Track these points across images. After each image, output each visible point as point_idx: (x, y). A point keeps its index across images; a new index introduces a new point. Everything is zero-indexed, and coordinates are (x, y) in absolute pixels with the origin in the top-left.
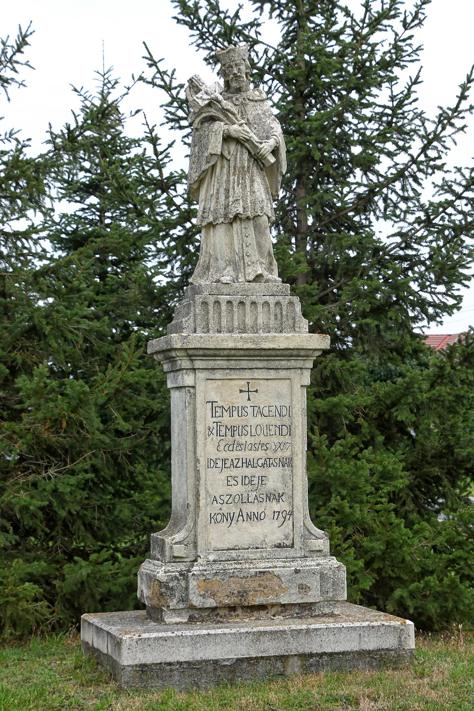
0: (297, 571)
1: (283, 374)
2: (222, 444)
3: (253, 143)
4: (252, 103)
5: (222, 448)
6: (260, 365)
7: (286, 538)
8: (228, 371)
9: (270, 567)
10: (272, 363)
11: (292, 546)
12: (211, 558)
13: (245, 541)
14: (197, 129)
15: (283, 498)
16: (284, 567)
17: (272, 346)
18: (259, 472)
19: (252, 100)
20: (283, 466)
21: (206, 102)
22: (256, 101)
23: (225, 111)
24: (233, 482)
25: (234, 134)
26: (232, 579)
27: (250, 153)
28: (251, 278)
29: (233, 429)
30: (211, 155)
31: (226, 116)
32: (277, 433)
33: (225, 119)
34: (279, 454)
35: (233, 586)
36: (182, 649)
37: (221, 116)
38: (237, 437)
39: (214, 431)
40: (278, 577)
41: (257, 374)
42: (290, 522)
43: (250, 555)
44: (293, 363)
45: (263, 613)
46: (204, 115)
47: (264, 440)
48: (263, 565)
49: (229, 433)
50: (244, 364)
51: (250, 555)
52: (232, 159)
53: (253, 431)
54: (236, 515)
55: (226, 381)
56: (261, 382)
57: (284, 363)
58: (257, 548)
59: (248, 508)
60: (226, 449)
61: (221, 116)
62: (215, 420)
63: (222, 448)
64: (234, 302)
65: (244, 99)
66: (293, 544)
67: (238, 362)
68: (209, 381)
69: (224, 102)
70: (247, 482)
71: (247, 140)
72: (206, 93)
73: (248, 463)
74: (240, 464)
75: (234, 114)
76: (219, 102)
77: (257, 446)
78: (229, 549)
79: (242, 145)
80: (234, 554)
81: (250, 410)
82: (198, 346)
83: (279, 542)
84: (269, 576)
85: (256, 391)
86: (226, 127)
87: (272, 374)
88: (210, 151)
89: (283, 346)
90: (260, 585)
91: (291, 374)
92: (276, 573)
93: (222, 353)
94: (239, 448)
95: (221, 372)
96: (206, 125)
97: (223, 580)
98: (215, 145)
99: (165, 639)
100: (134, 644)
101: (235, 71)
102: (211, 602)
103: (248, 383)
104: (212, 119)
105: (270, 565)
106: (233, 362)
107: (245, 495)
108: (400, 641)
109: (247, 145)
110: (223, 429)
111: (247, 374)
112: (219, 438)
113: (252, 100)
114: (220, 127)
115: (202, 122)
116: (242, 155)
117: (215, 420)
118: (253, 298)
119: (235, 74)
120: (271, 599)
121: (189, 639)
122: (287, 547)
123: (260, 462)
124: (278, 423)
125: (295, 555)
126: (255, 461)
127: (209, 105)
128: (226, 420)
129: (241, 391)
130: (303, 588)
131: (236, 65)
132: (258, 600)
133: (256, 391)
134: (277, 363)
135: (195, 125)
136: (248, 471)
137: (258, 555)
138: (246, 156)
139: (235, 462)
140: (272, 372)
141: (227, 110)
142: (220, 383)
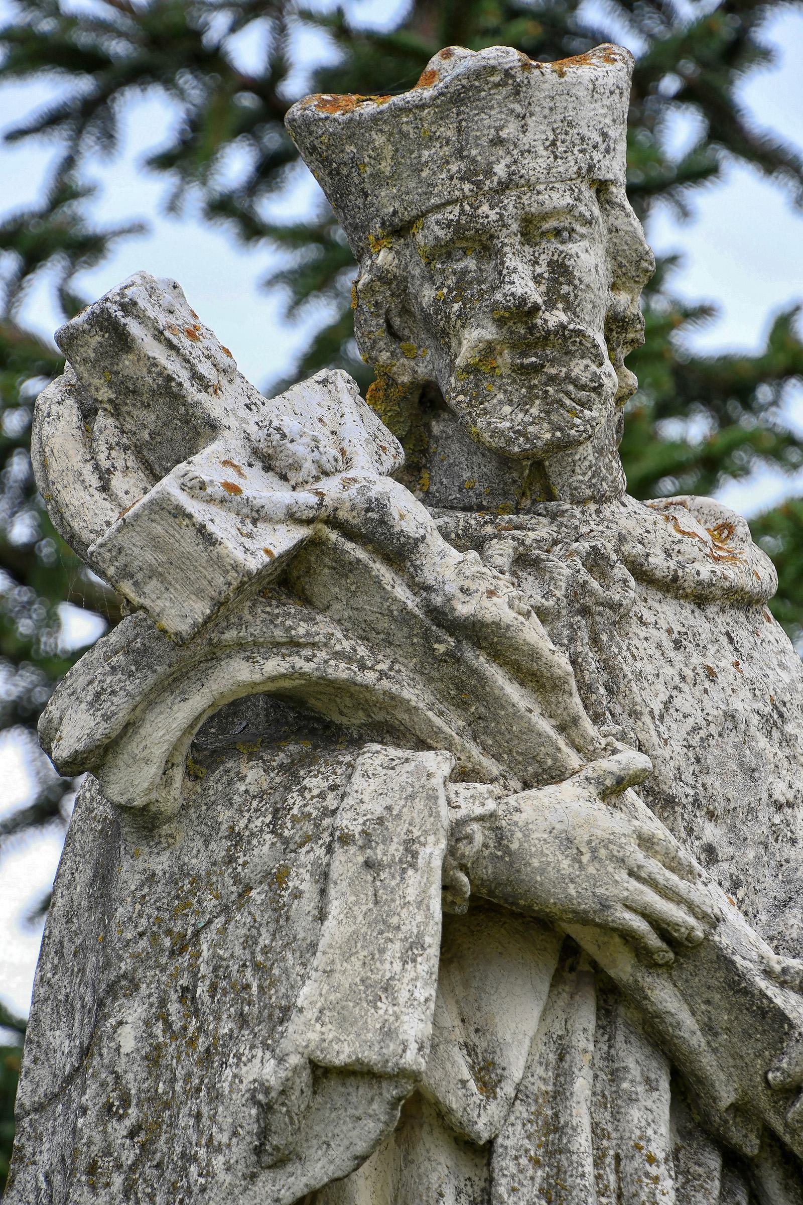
3: (735, 984)
4: (670, 614)
14: (144, 821)
19: (670, 586)
21: (283, 539)
22: (700, 598)
23: (453, 642)
25: (557, 876)
27: (686, 1090)
30: (321, 1073)
31: (466, 693)
33: (450, 724)
37: (416, 694)
46: (239, 673)
52: (516, 1140)
61: (416, 694)
65: (596, 561)
69: (444, 563)
71: (682, 950)
72: (268, 460)
76: (400, 553)
79: (612, 998)
86: (475, 800)
88: (305, 1034)
96: (254, 776)
98: (369, 981)
101: (523, 282)
104: (309, 723)
109: (665, 996)
113: (670, 586)
114: (404, 798)
115: (210, 748)
116: (611, 1100)
119: (524, 312)
127: (288, 579)
131: (531, 229)
135: (137, 778)
138: (651, 1118)
141: (479, 634)
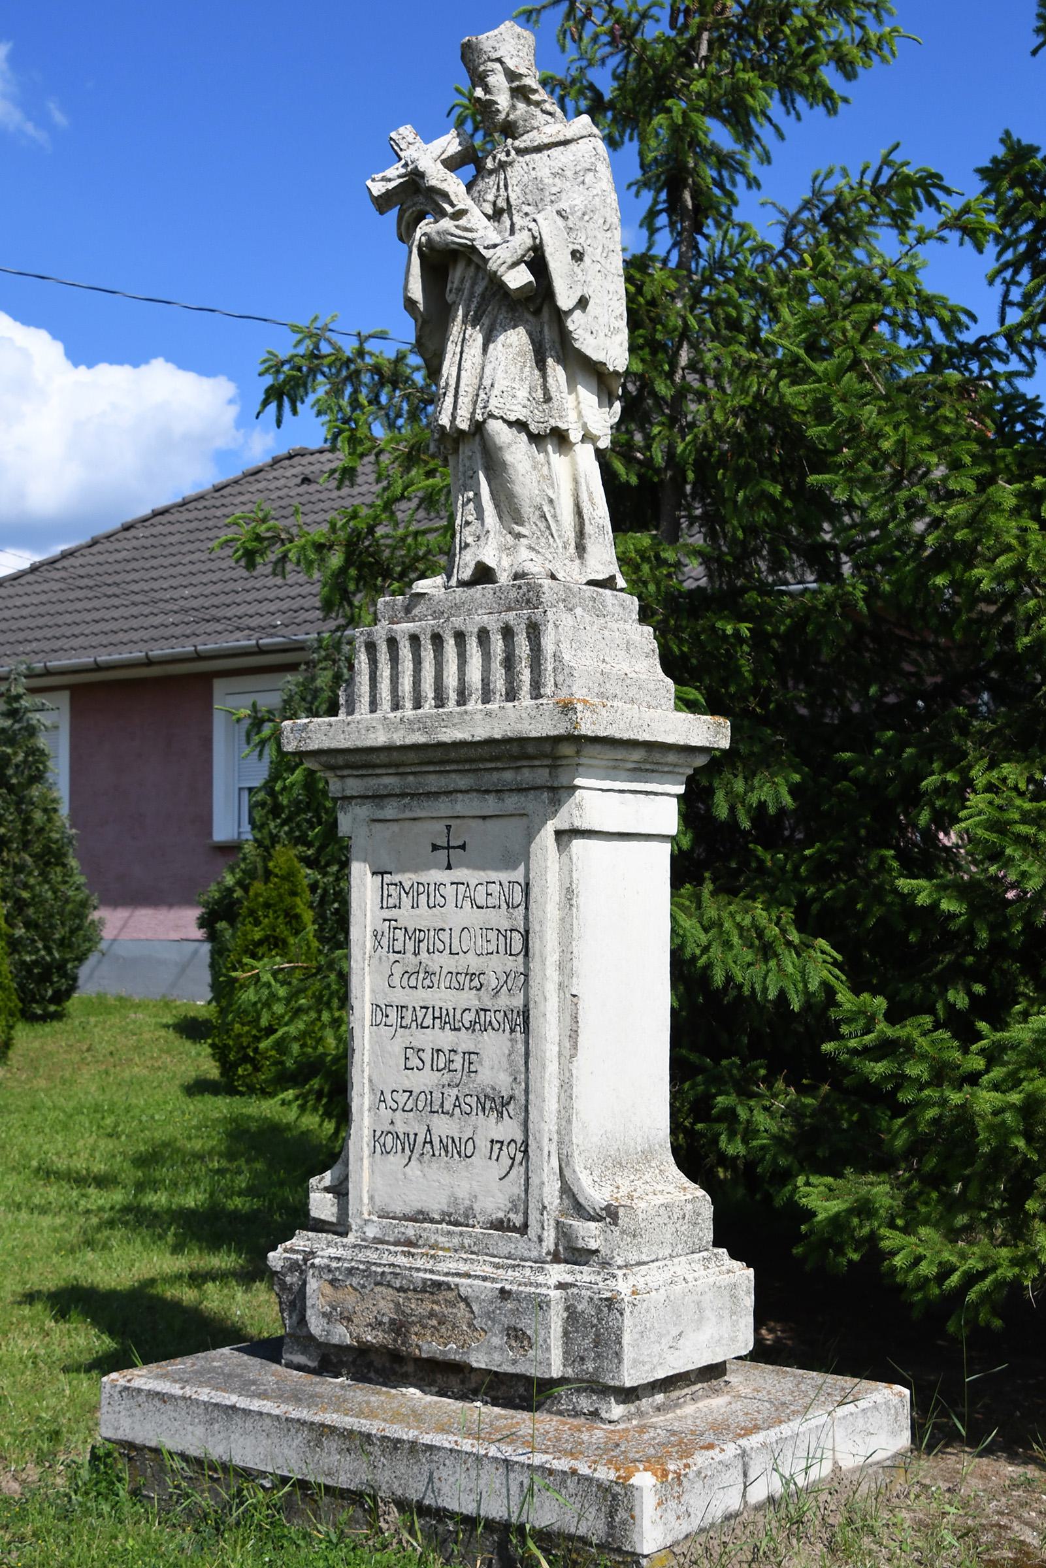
0: (504, 1294)
1: (511, 802)
2: (398, 970)
5: (396, 980)
6: (463, 782)
7: (514, 1209)
8: (407, 800)
9: (458, 1275)
10: (487, 776)
11: (523, 1229)
12: (371, 1232)
13: (436, 1204)
15: (511, 1107)
16: (485, 1279)
17: (458, 735)
18: (465, 1041)
20: (512, 1031)
24: (415, 1062)
26: (378, 1289)
28: (466, 574)
29: (417, 936)
32: (502, 949)
34: (504, 1001)
35: (382, 1303)
36: (190, 1428)
38: (424, 955)
39: (384, 942)
40: (465, 1300)
41: (466, 805)
42: (522, 1169)
43: (441, 1239)
44: (527, 776)
45: (454, 1382)
47: (473, 962)
48: (452, 1266)
49: (410, 946)
50: (434, 782)
51: (441, 1239)
53: (455, 941)
54: (420, 1139)
55: (407, 824)
56: (474, 823)
57: (508, 776)
58: (456, 1224)
59: (443, 1127)
60: (404, 983)
62: (387, 914)
63: (396, 980)
64: (422, 637)
66: (526, 1225)
67: (421, 779)
68: (379, 826)
70: (441, 1065)
73: (445, 1019)
74: (428, 1021)
75: (445, 196)
77: (461, 978)
78: (406, 1218)
80: (411, 1229)
81: (449, 891)
82: (326, 745)
83: (501, 1215)
84: (451, 1295)
85: (463, 847)
87: (491, 805)
89: (481, 734)
90: (432, 1314)
91: (529, 803)
92: (463, 1291)
93: (374, 758)
94: (427, 982)
95: (394, 803)
97: (364, 1287)
99: (162, 1397)
100: (116, 1396)
102: (341, 1335)
103: (448, 827)
105: (463, 1268)
106: (411, 778)
107: (437, 1095)
108: (611, 1526)
110: (399, 934)
111: (443, 807)
112: (393, 957)
117: (387, 914)
118: (457, 622)
120: (451, 1351)
121: (201, 1410)
122: (514, 1229)
123: (469, 1017)
124: (505, 925)
125: (526, 1254)
126: (458, 1017)
128: (407, 916)
129: (435, 847)
130: (516, 1335)
132: (430, 1346)
133: (463, 847)
134: (495, 776)
136: (445, 1038)
137: (456, 1241)
139: (420, 1014)
140: (491, 799)
142: (395, 827)
